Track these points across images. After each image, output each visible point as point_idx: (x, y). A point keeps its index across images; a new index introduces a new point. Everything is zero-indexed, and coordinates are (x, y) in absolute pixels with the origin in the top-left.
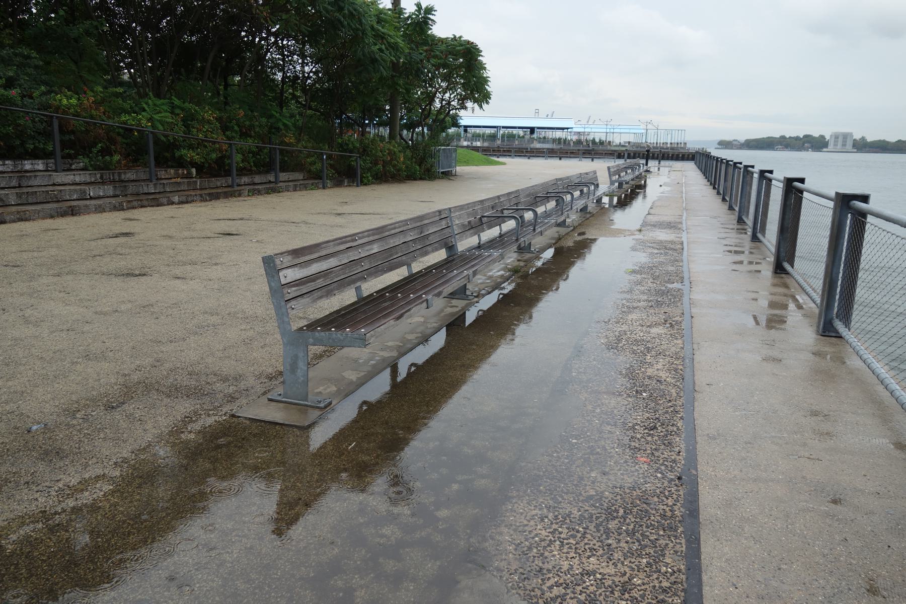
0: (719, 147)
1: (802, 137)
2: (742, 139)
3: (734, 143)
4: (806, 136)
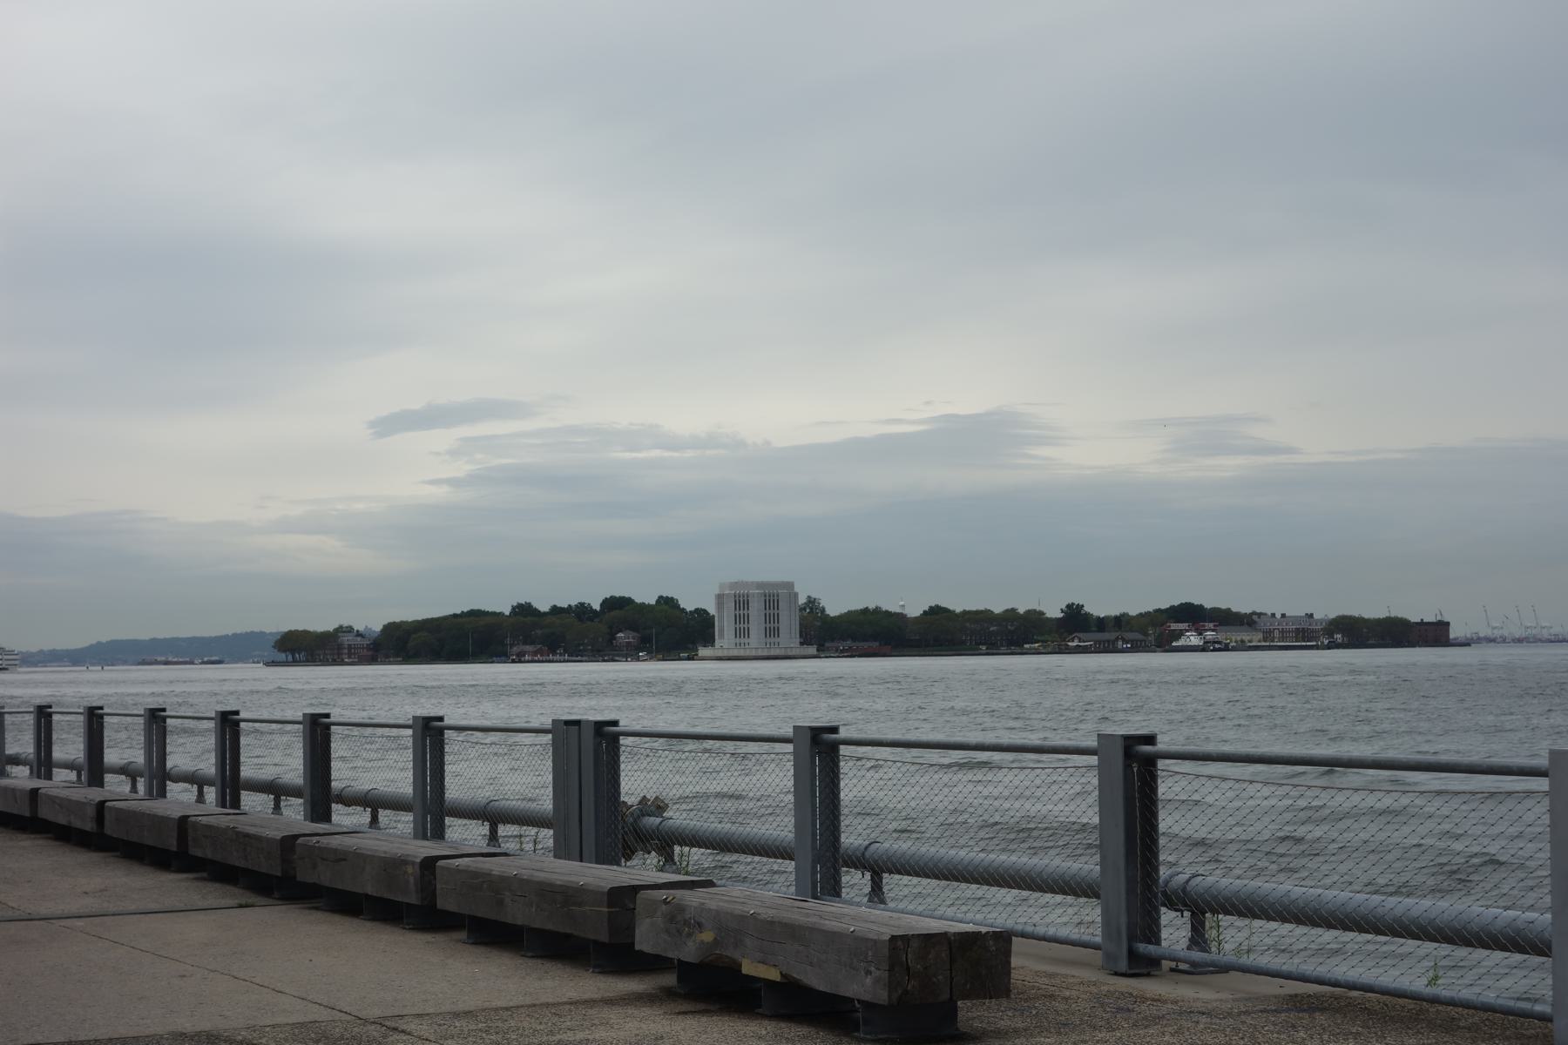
0: (282, 657)
1: (597, 607)
2: (372, 621)
3: (346, 639)
4: (613, 604)
